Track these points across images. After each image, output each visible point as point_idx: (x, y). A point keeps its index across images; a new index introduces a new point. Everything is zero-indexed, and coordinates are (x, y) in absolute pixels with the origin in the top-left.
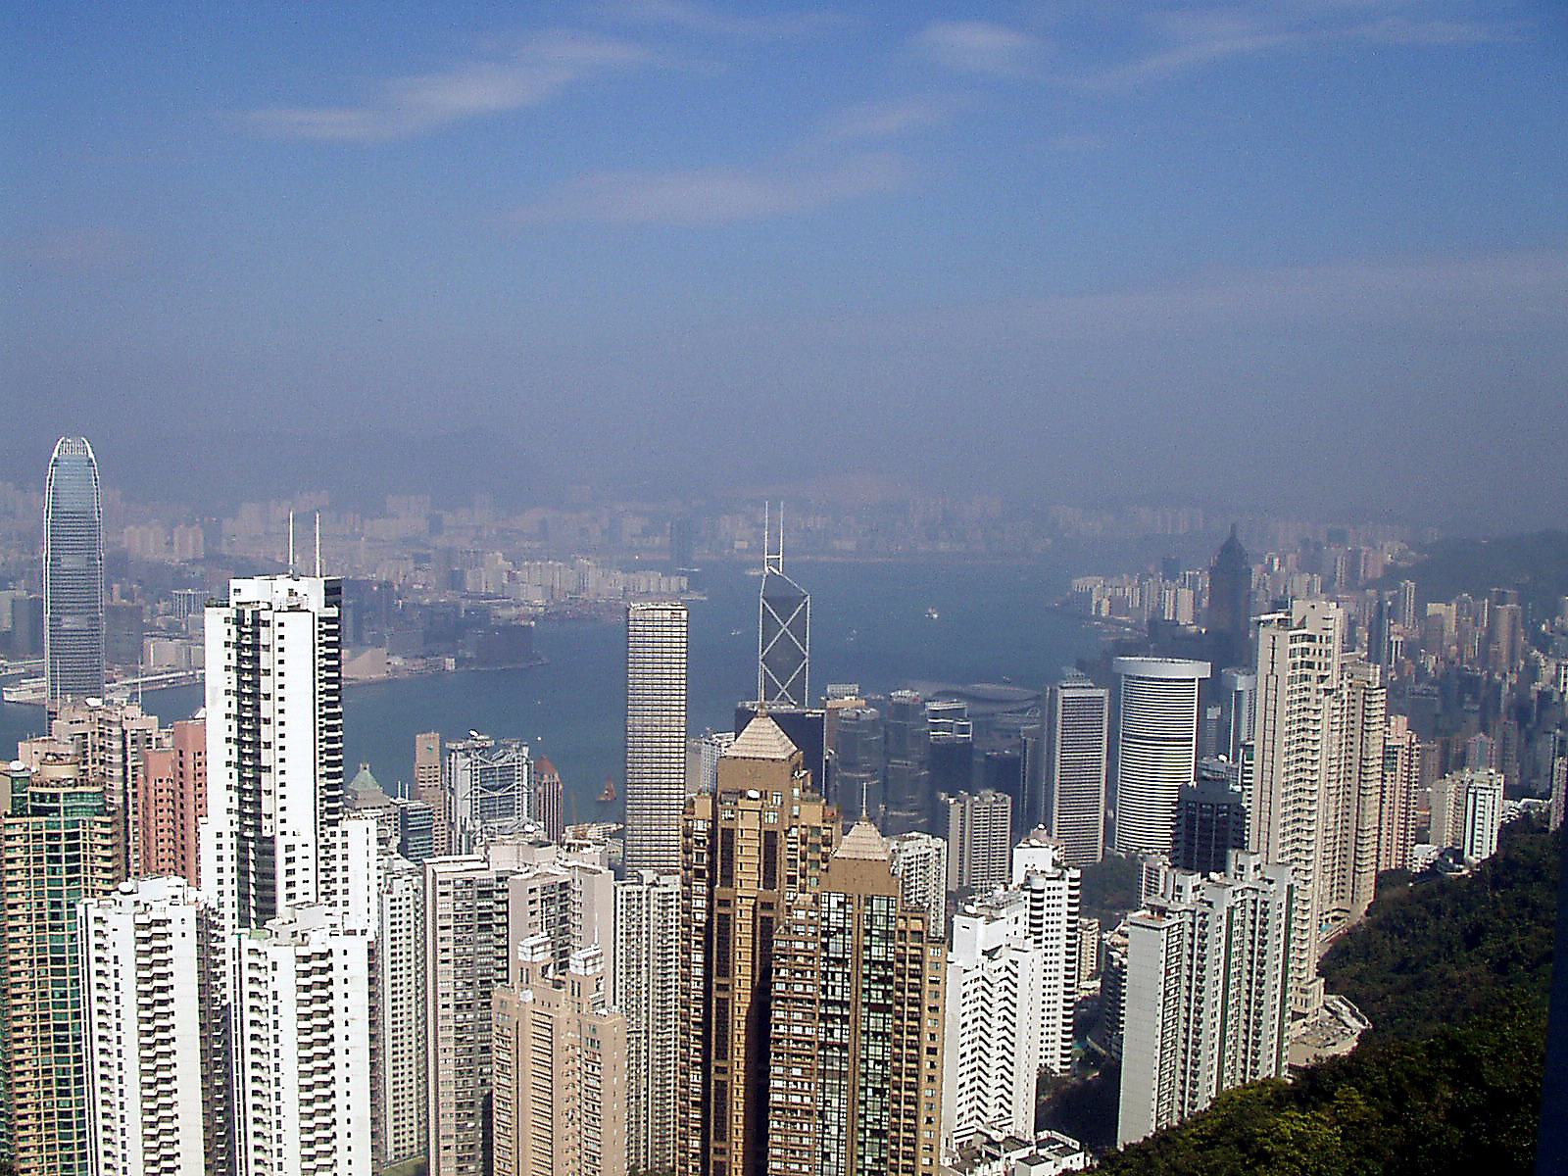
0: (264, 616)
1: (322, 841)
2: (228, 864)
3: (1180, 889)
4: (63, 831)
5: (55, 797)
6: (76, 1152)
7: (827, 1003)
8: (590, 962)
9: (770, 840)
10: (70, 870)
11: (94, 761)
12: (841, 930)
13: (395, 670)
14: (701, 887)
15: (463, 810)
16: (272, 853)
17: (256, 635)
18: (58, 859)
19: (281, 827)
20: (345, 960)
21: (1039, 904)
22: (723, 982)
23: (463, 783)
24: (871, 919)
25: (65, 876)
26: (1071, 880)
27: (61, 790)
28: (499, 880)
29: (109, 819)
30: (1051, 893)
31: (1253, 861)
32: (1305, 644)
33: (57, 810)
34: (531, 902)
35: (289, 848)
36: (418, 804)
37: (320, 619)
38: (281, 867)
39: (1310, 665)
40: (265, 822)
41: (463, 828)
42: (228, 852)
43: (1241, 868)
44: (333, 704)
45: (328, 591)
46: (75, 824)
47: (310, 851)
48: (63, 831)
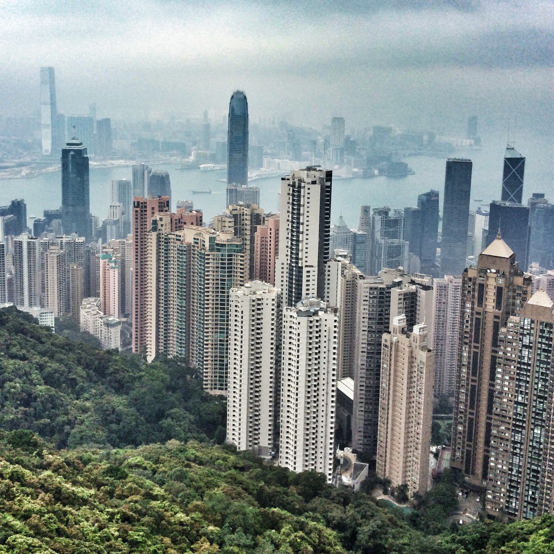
0: (303, 184)
2: (285, 275)
4: (227, 258)
5: (225, 245)
6: (224, 375)
8: (421, 330)
11: (240, 225)
14: (468, 305)
15: (378, 235)
17: (299, 192)
18: (224, 268)
20: (326, 323)
22: (477, 345)
23: (378, 227)
25: (226, 274)
28: (389, 288)
29: (242, 254)
34: (400, 299)
35: (308, 272)
36: (361, 232)
38: (304, 279)
40: (300, 261)
41: (377, 242)
42: (285, 270)
46: (231, 255)
47: (316, 273)
48: (227, 258)
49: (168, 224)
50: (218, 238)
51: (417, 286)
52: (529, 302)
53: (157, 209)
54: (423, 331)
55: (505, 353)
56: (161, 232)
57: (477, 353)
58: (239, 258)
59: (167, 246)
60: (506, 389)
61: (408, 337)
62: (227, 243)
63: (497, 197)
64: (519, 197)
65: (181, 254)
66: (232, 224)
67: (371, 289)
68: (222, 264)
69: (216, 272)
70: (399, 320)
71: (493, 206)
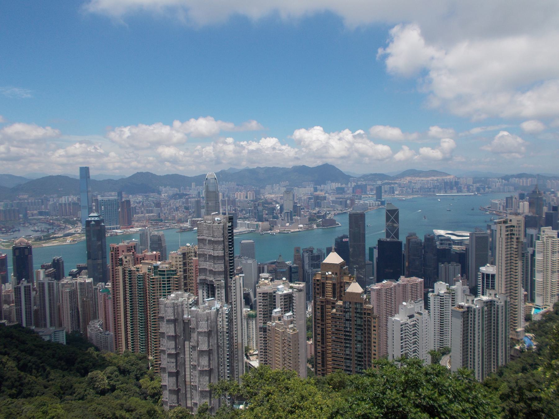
3: (468, 300)
4: (166, 280)
5: (164, 271)
9: (334, 285)
10: (168, 289)
12: (349, 311)
13: (301, 228)
15: (307, 267)
18: (165, 287)
21: (442, 300)
23: (307, 261)
24: (356, 309)
26: (452, 293)
32: (512, 228)
33: (164, 275)
36: (295, 265)
39: (514, 234)
41: (307, 271)
43: (490, 294)
48: (166, 280)
50: (161, 266)
53: (125, 250)
54: (290, 317)
56: (126, 266)
57: (323, 328)
59: (130, 276)
62: (166, 269)
63: (384, 238)
64: (397, 235)
65: (139, 281)
66: (181, 259)
67: (263, 294)
68: (163, 284)
70: (276, 312)
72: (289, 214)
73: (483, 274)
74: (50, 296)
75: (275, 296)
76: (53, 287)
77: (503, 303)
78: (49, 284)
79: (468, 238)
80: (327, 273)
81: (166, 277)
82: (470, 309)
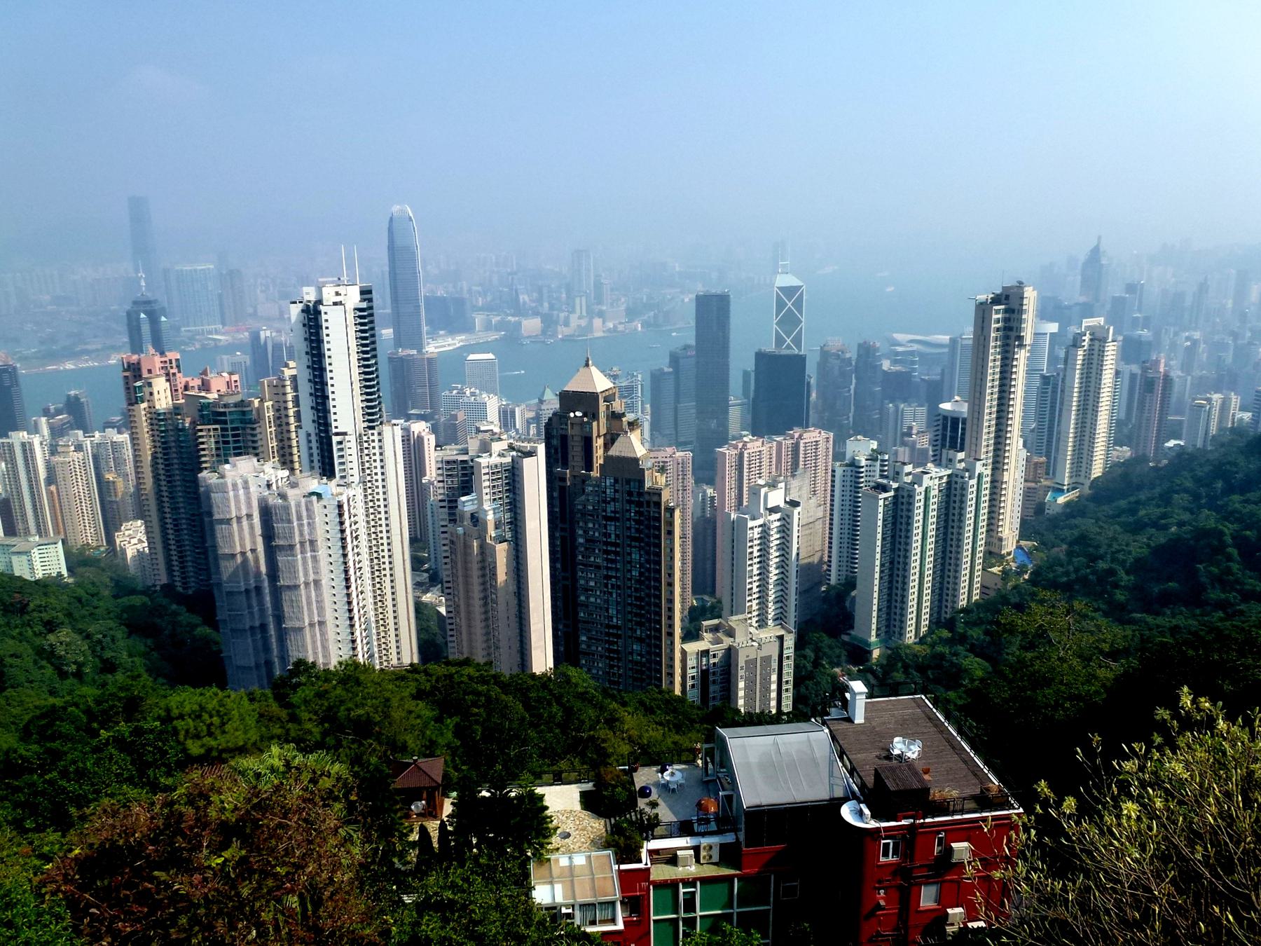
1: (365, 438)
5: (224, 414)
7: (606, 544)
12: (614, 500)
16: (330, 445)
19: (334, 431)
27: (227, 410)
30: (868, 469)
31: (961, 455)
33: (226, 423)
35: (340, 443)
37: (355, 309)
38: (336, 455)
44: (367, 359)
45: (362, 293)
46: (237, 429)
48: (230, 433)
49: (162, 392)
51: (514, 453)
52: (610, 453)
55: (585, 532)
58: (249, 431)
60: (592, 584)
61: (475, 526)
62: (227, 410)
64: (798, 341)
67: (448, 462)
69: (218, 455)
70: (464, 502)
71: (760, 356)
72: (584, 299)
73: (945, 418)
74: (28, 472)
75: (472, 467)
76: (32, 451)
77: (974, 482)
78: (23, 445)
79: (946, 350)
80: (572, 415)
81: (229, 426)
82: (901, 493)
